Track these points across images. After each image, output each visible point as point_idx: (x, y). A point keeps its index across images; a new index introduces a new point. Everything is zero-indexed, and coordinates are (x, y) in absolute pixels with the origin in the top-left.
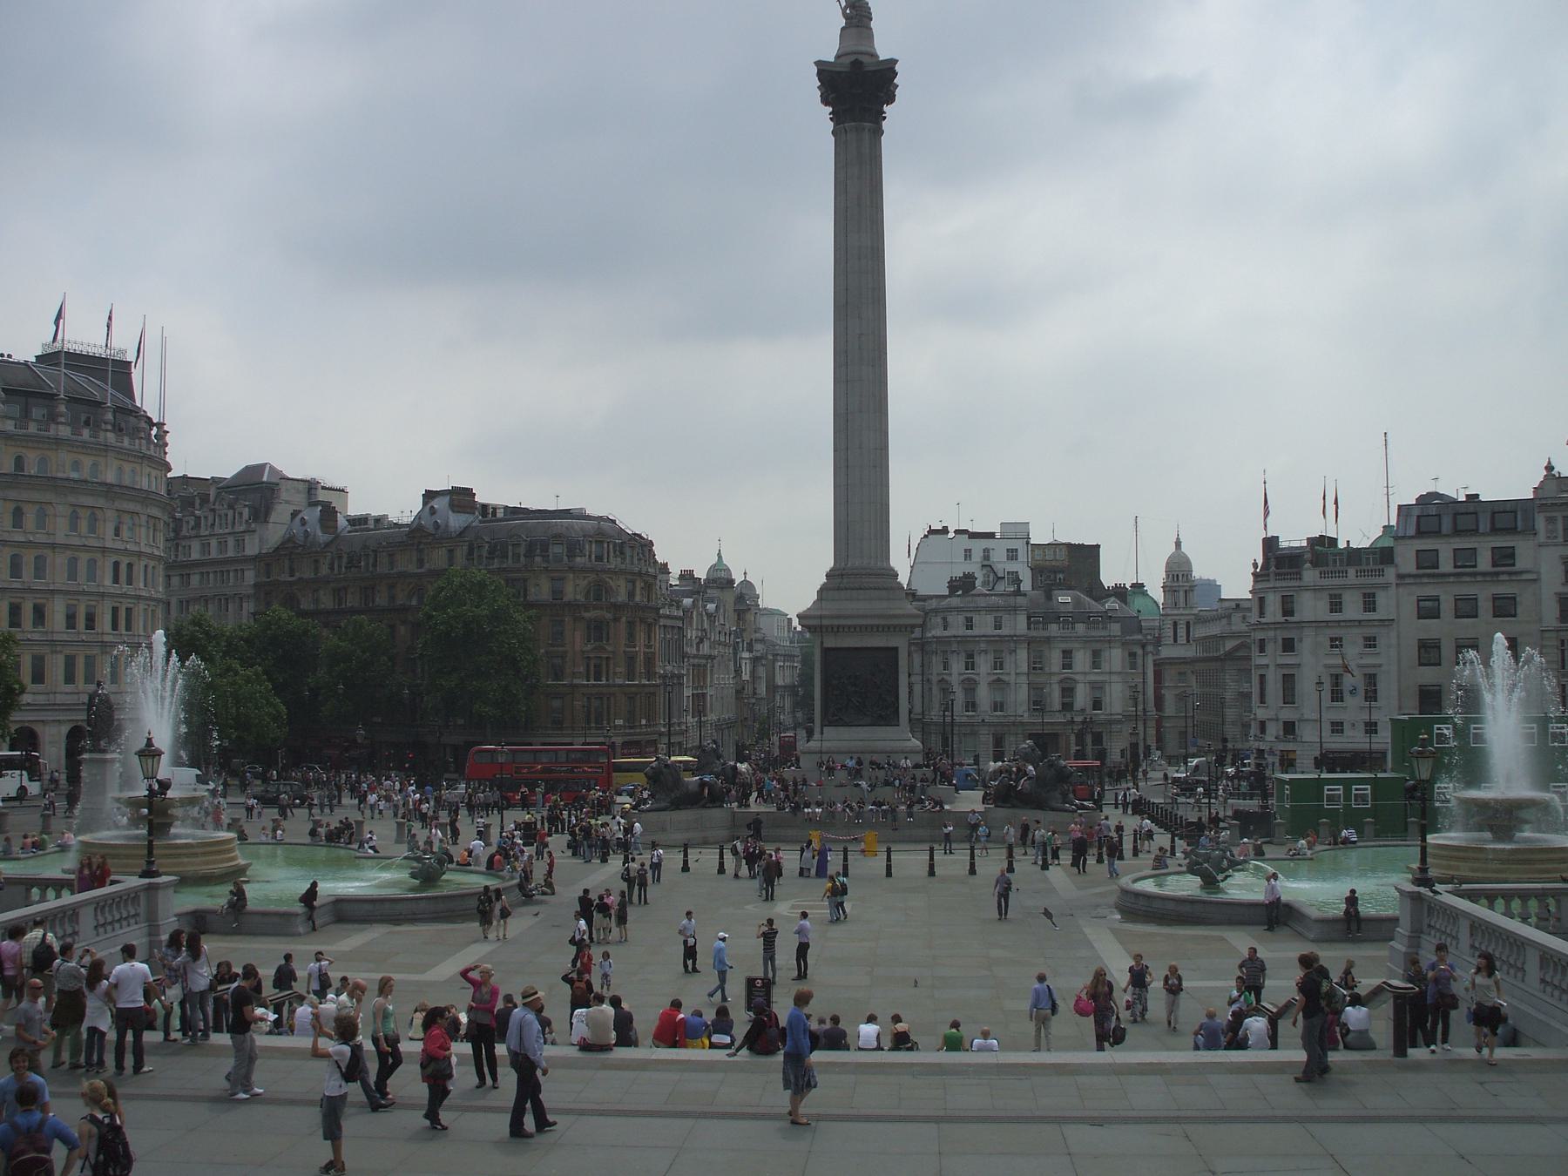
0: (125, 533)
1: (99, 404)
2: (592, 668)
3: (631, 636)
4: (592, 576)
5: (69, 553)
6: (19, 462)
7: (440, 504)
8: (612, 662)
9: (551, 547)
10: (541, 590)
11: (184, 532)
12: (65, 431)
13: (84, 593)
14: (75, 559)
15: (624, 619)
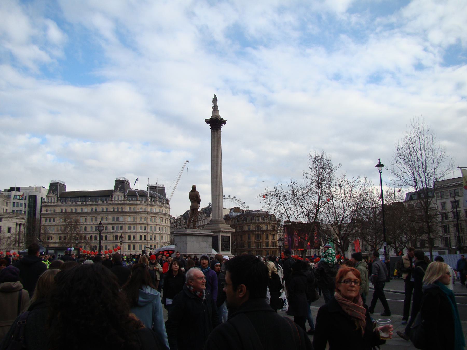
0: (153, 220)
1: (147, 196)
2: (257, 245)
3: (267, 238)
4: (256, 224)
5: (139, 225)
6: (130, 208)
7: (232, 211)
8: (262, 243)
9: (247, 219)
10: (246, 228)
11: (198, 220)
12: (139, 202)
13: (143, 233)
14: (142, 226)
15: (265, 234)
